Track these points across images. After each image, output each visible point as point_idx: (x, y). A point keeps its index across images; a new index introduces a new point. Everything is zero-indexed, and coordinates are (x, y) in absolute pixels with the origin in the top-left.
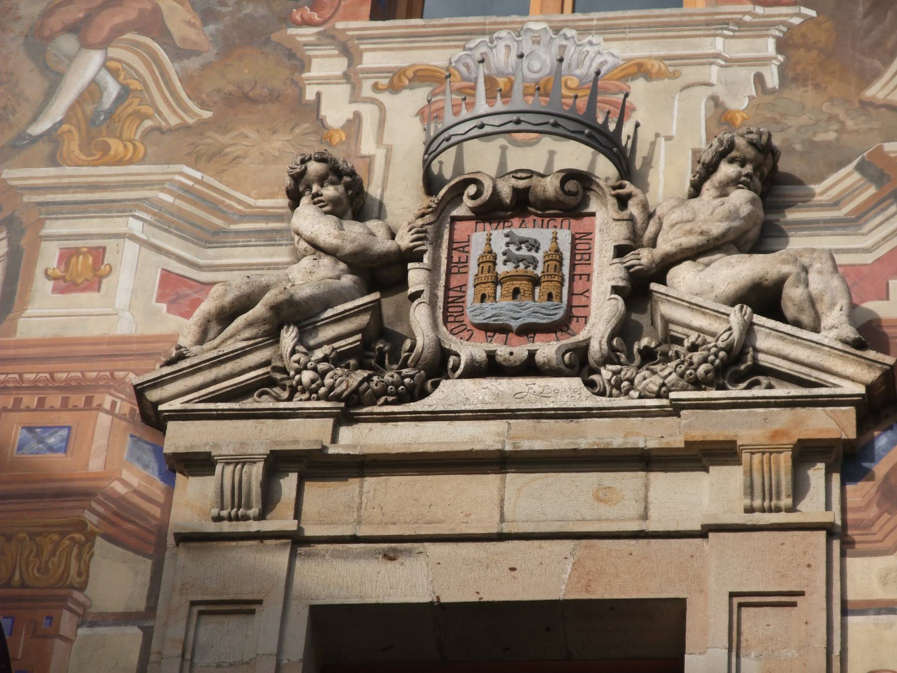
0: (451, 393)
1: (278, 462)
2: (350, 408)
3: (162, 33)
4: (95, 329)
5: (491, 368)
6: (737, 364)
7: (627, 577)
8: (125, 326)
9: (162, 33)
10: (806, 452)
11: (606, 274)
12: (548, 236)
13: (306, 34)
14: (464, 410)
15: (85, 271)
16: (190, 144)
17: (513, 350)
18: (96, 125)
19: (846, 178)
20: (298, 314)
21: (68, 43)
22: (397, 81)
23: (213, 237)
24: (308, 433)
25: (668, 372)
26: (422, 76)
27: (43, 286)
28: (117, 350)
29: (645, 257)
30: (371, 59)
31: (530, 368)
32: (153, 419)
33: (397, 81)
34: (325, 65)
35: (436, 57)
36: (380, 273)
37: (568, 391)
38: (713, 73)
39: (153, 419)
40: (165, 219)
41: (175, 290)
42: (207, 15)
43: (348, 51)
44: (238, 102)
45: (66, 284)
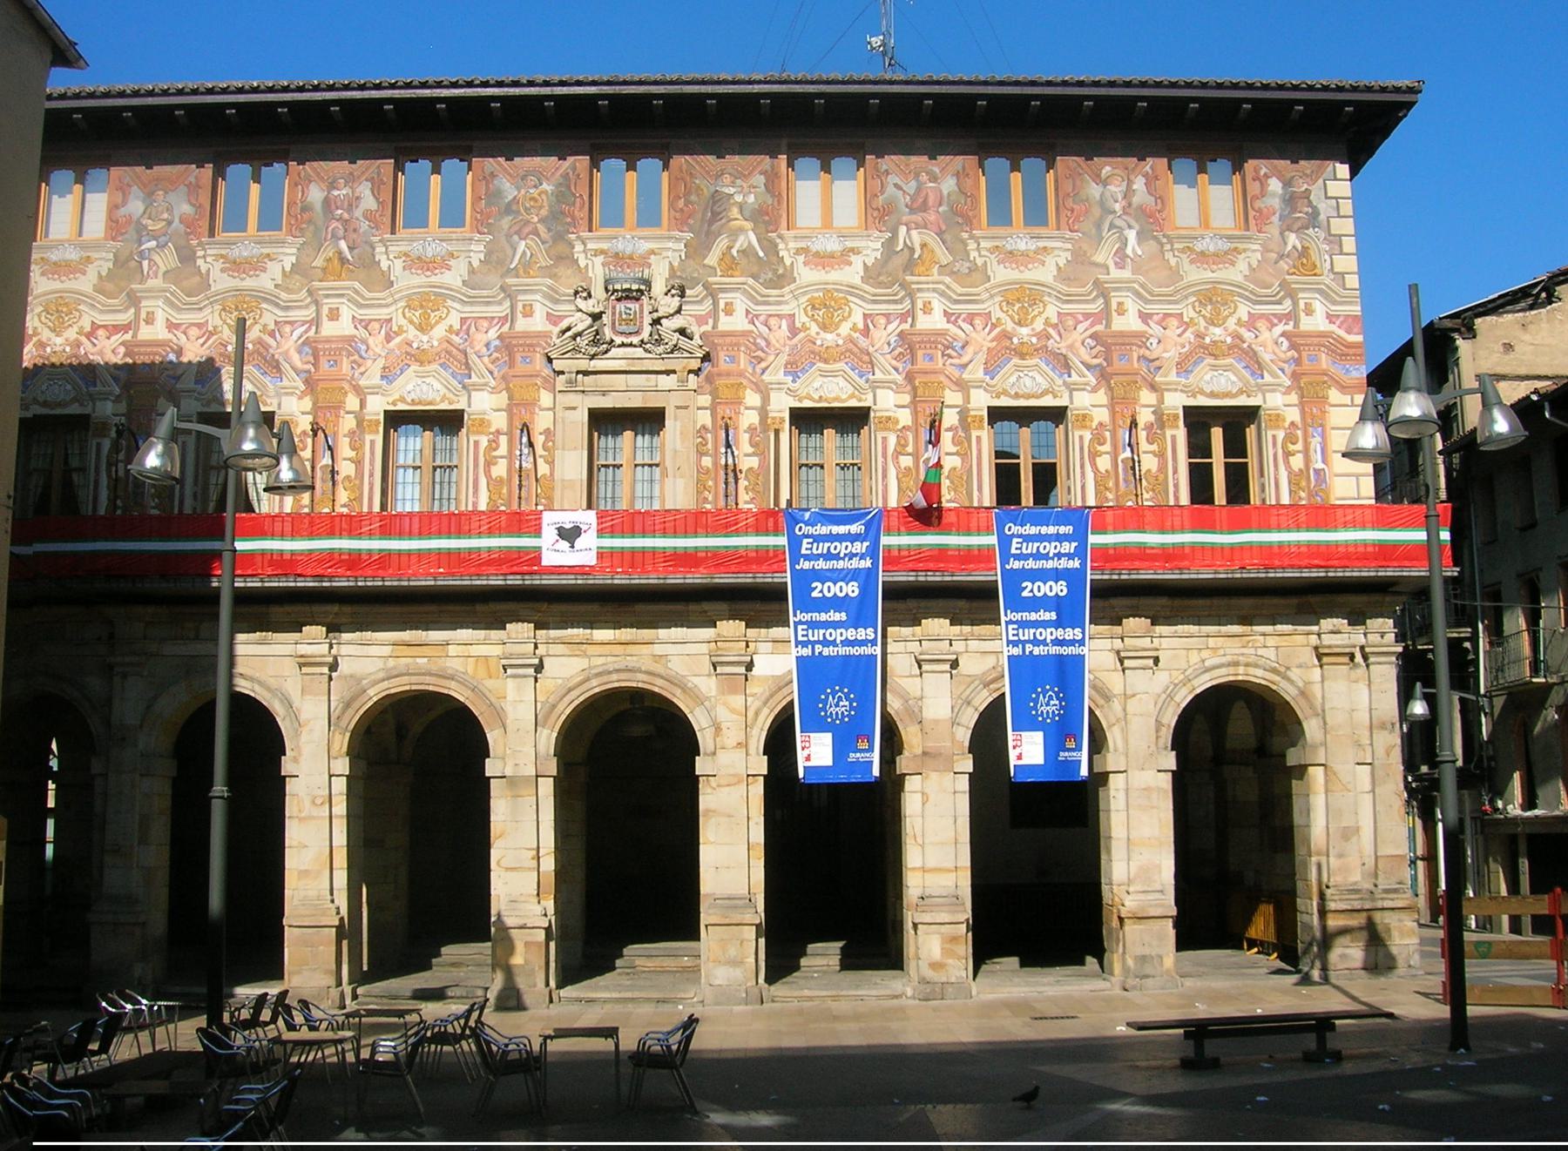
0: (614, 352)
1: (578, 372)
2: (593, 357)
3: (538, 236)
4: (533, 329)
5: (623, 345)
6: (675, 348)
7: (653, 402)
8: (539, 329)
9: (538, 236)
10: (690, 372)
11: (647, 320)
12: (634, 306)
13: (573, 236)
14: (616, 359)
15: (528, 313)
16: (548, 272)
17: (626, 341)
18: (527, 266)
19: (700, 288)
20: (580, 334)
21: (516, 238)
22: (597, 253)
23: (557, 302)
24: (584, 364)
25: (661, 349)
26: (602, 252)
27: (520, 315)
28: (539, 335)
29: (655, 315)
30: (589, 246)
31: (631, 345)
32: (550, 360)
33: (597, 253)
34: (579, 247)
35: (605, 246)
36: (596, 317)
37: (639, 352)
38: (670, 254)
39: (550, 360)
40: (546, 296)
41: (553, 319)
42: (549, 230)
43: (584, 244)
44: (560, 259)
45: (525, 315)
